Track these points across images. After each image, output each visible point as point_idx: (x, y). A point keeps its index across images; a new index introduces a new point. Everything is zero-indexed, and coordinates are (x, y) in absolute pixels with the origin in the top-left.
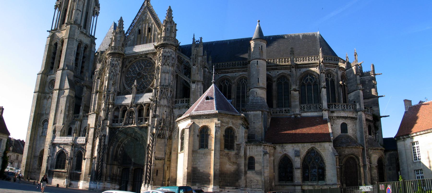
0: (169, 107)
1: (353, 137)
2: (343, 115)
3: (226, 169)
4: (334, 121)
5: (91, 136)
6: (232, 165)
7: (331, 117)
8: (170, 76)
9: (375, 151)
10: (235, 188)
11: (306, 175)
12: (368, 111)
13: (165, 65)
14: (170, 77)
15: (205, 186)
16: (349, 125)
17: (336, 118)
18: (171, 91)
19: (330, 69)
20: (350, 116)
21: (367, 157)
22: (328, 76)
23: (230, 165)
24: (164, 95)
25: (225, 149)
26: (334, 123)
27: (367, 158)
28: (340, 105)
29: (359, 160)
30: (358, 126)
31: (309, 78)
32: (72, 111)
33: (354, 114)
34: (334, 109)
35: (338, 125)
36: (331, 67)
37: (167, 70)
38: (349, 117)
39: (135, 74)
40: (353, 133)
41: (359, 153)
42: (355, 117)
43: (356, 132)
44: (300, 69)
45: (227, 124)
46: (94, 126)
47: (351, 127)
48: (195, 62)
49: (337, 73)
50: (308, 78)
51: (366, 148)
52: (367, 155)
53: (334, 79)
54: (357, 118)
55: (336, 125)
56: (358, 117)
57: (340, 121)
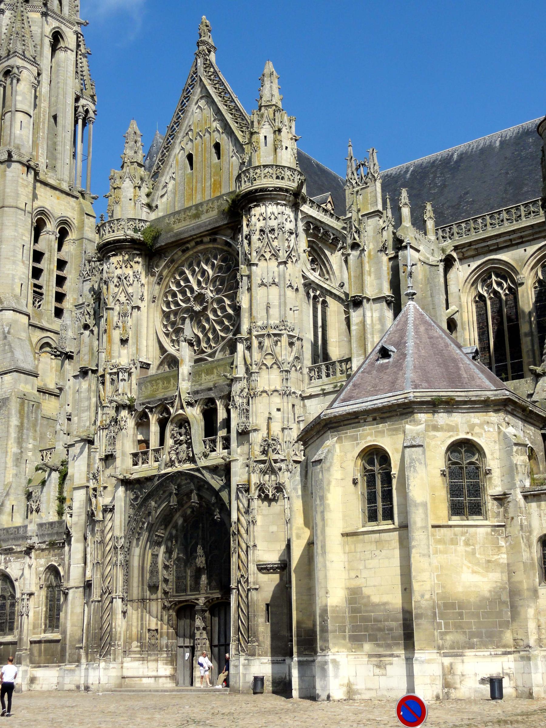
0: (286, 394)
3: (460, 589)
5: (79, 516)
6: (481, 570)
8: (282, 293)
10: (500, 651)
13: (266, 260)
14: (282, 297)
15: (395, 653)
18: (291, 344)
23: (474, 572)
24: (269, 357)
25: (454, 518)
32: (31, 441)
37: (271, 275)
39: (187, 300)
45: (451, 433)
48: (356, 236)
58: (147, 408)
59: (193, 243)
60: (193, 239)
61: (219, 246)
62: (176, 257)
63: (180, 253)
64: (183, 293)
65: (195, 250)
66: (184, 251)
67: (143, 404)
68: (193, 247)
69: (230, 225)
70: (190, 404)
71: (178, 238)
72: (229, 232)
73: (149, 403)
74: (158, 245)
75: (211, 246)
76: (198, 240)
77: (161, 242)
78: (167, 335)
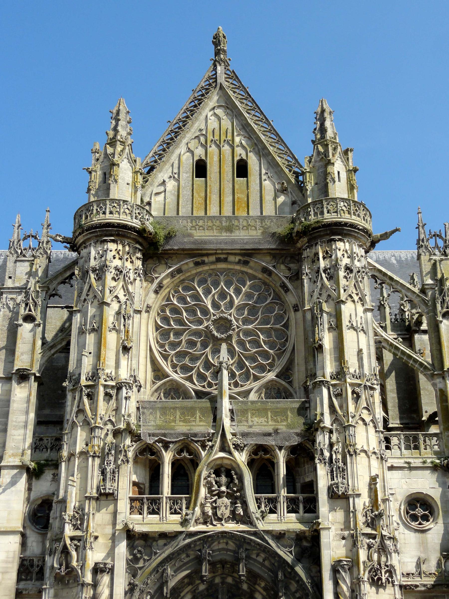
46: (18, 525)
58: (160, 441)
59: (213, 258)
60: (216, 254)
61: (250, 271)
62: (184, 268)
63: (192, 265)
64: (191, 311)
65: (213, 267)
66: (197, 264)
67: (154, 435)
68: (212, 263)
69: (272, 252)
70: (237, 447)
71: (200, 247)
72: (268, 258)
73: (164, 435)
74: (168, 247)
75: (238, 267)
76: (222, 256)
77: (174, 245)
78: (165, 358)
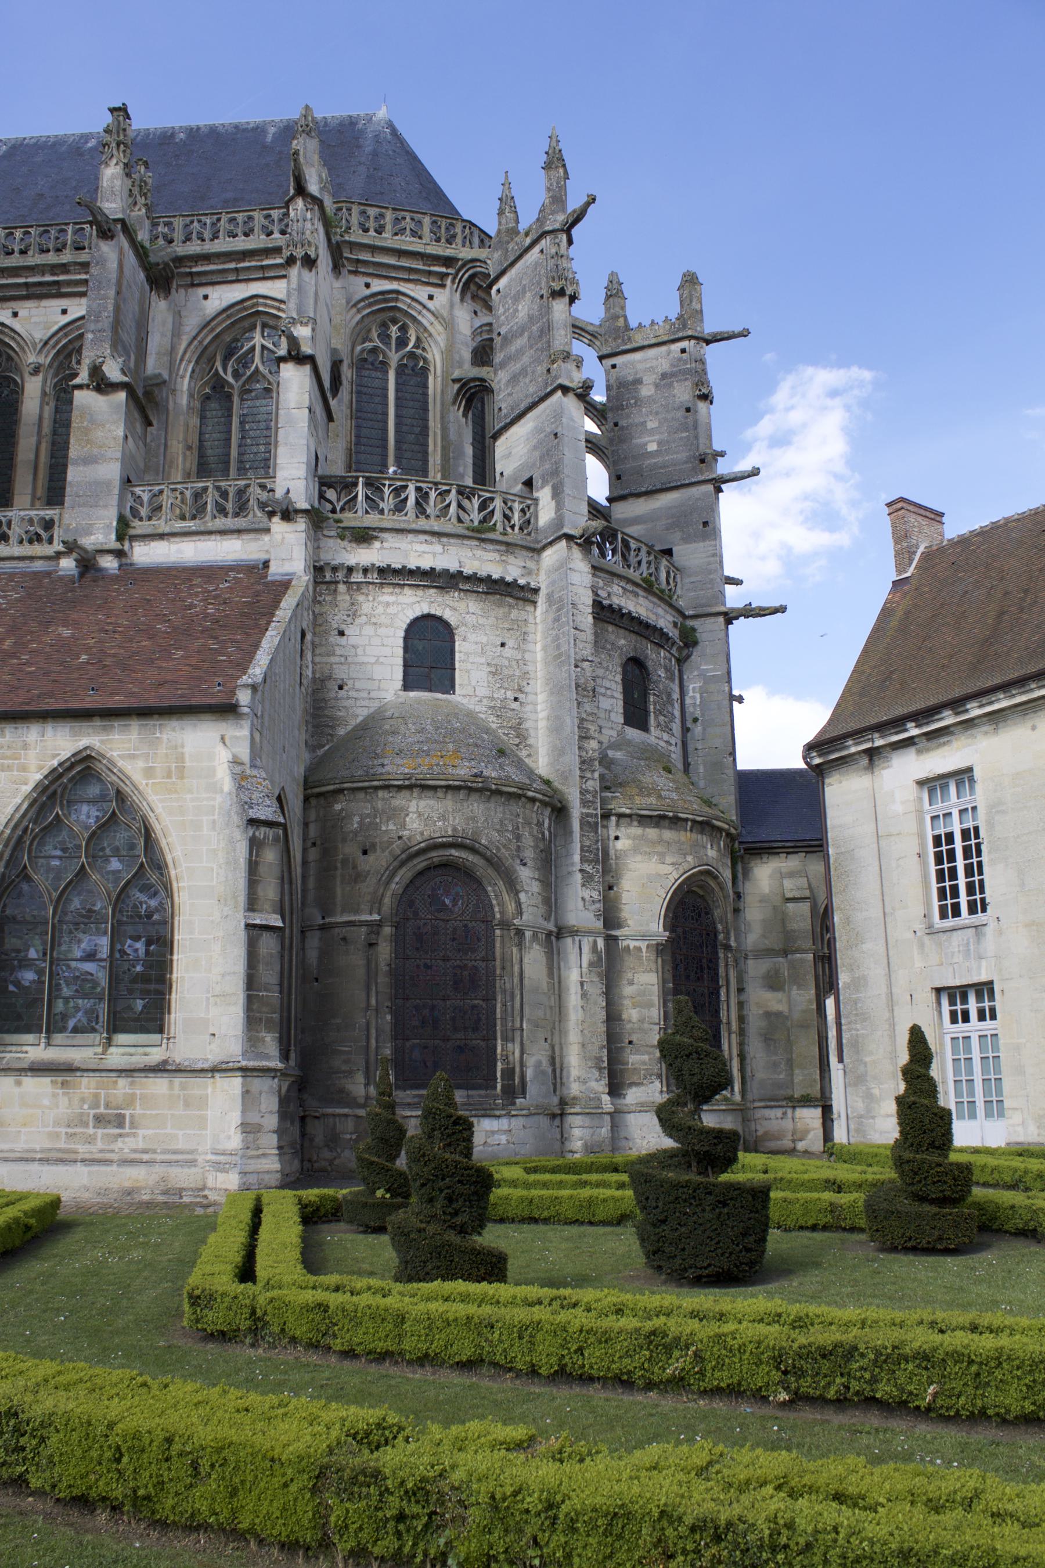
1: (493, 722)
2: (426, 564)
4: (361, 598)
7: (335, 569)
9: (652, 833)
11: (17, 984)
12: (633, 559)
16: (472, 637)
17: (373, 577)
19: (398, 292)
20: (483, 573)
21: (588, 868)
22: (385, 337)
26: (354, 615)
27: (587, 879)
28: (411, 487)
29: (513, 885)
30: (539, 646)
31: (258, 349)
33: (511, 559)
34: (360, 517)
35: (382, 631)
36: (412, 276)
38: (474, 578)
40: (499, 694)
41: (518, 838)
42: (522, 582)
43: (520, 691)
44: (208, 290)
47: (483, 653)
49: (449, 325)
50: (253, 348)
51: (584, 803)
52: (583, 860)
53: (425, 360)
54: (536, 591)
55: (368, 630)
56: (542, 581)
57: (401, 599)
